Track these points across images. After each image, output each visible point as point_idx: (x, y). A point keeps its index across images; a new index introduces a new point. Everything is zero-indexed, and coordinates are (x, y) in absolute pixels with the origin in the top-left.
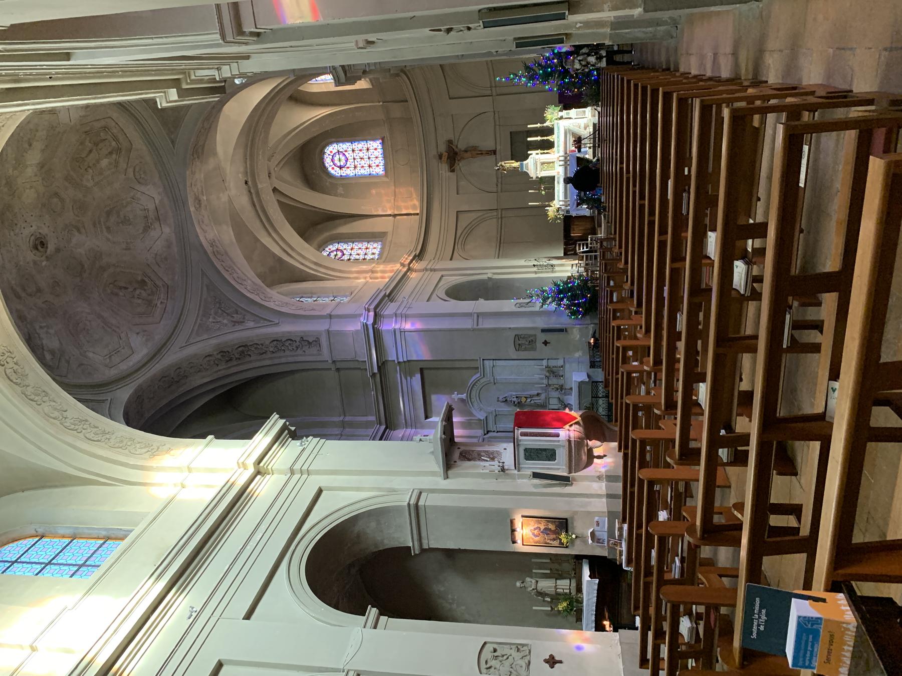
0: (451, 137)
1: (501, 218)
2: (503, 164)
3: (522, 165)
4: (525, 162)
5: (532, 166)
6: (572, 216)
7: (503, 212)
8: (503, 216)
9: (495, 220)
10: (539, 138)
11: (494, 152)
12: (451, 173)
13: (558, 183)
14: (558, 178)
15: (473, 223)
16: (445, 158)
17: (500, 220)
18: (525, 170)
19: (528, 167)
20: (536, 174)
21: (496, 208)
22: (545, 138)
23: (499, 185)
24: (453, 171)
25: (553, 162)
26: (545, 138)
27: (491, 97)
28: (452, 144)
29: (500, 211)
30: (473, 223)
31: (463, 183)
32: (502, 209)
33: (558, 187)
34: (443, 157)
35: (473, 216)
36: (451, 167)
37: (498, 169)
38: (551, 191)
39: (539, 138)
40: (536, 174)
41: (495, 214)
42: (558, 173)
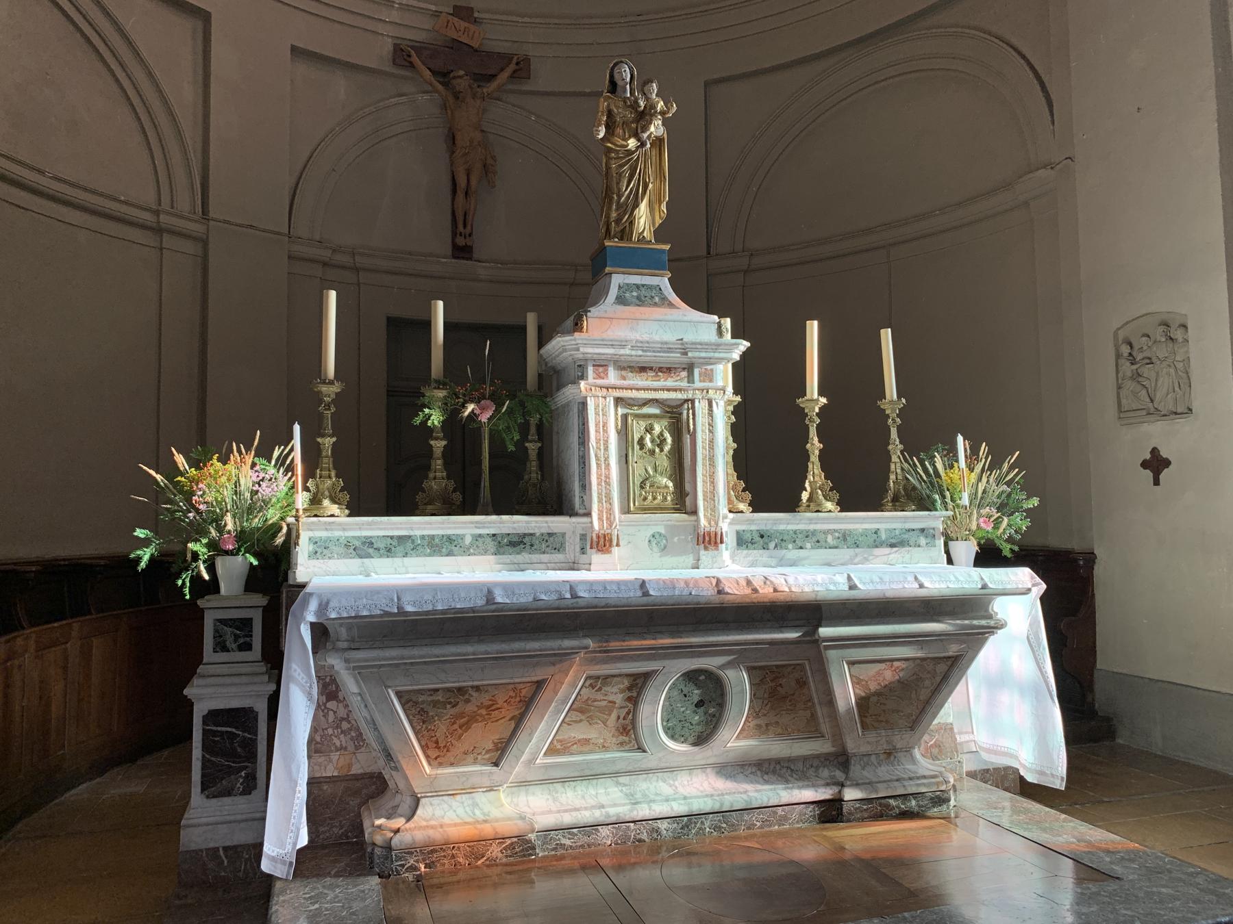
0: (543, 79)
1: (159, 231)
2: (656, 128)
3: (640, 260)
4: (664, 282)
5: (670, 336)
6: (188, 674)
7: (189, 247)
8: (168, 241)
9: (149, 198)
10: (814, 397)
11: (462, 251)
12: (389, 47)
13: (518, 543)
14: (552, 542)
15: (140, 76)
16: (460, 31)
17: (147, 217)
18: (617, 280)
19: (640, 302)
20: (601, 365)
21: (212, 214)
22: (815, 445)
23: (326, 254)
24: (402, 55)
25: (683, 501)
26: (815, 445)
27: (705, 253)
28: (512, 76)
29: (196, 228)
30: (140, 76)
31: (340, 86)
32: (205, 243)
33: (478, 545)
34: (463, 24)
35: (184, 94)
36: (419, 48)
37: (613, 87)
38: (438, 479)
39: (814, 397)
40: (601, 365)
41: (184, 204)
42: (604, 543)
